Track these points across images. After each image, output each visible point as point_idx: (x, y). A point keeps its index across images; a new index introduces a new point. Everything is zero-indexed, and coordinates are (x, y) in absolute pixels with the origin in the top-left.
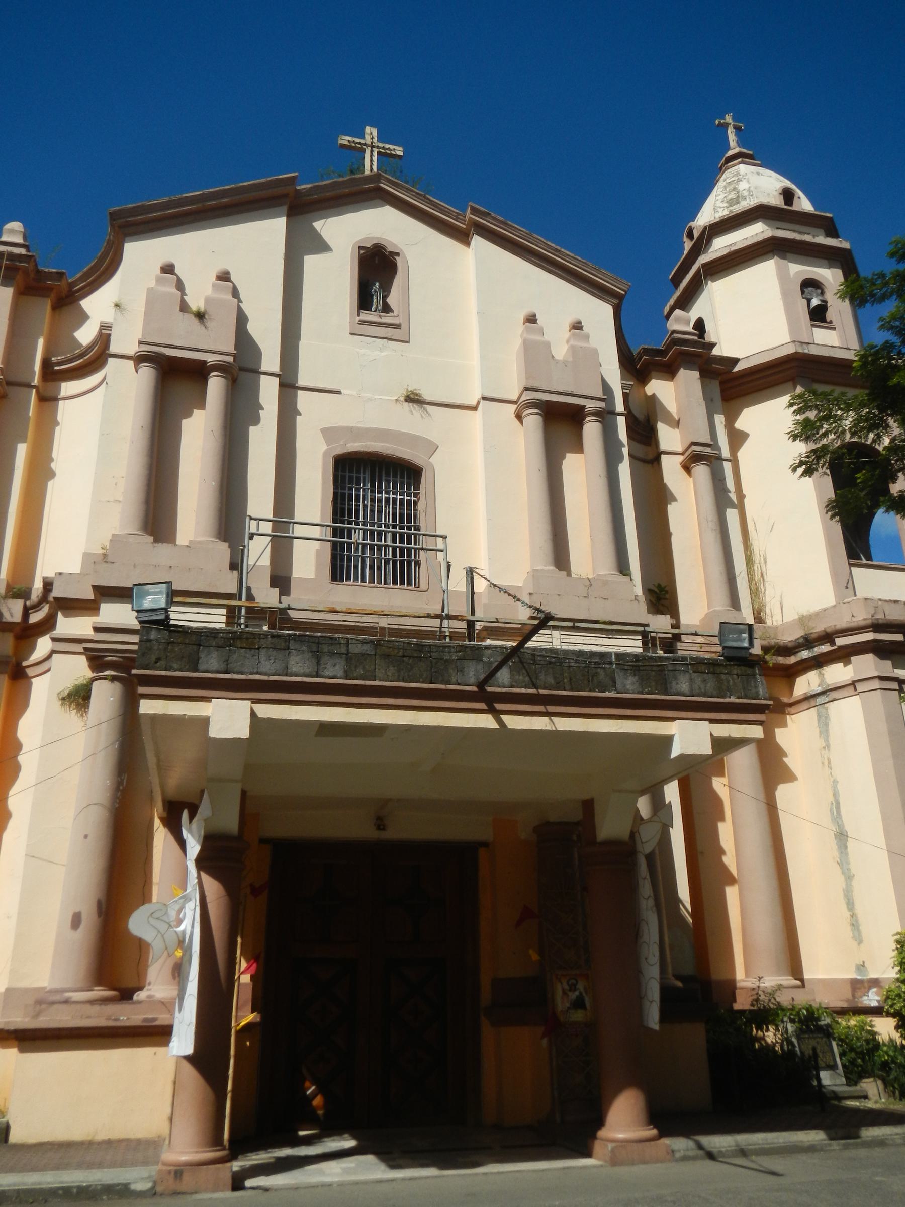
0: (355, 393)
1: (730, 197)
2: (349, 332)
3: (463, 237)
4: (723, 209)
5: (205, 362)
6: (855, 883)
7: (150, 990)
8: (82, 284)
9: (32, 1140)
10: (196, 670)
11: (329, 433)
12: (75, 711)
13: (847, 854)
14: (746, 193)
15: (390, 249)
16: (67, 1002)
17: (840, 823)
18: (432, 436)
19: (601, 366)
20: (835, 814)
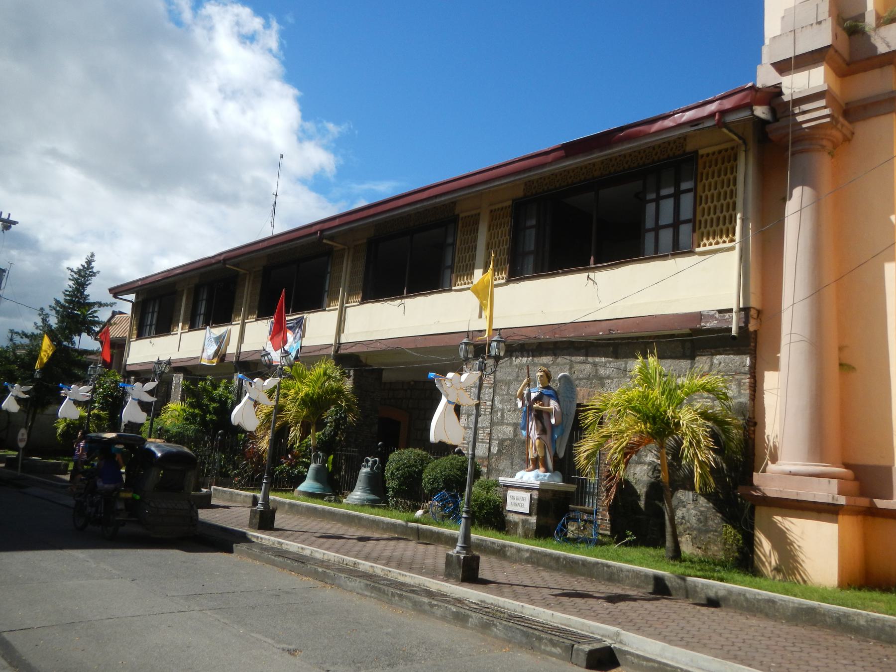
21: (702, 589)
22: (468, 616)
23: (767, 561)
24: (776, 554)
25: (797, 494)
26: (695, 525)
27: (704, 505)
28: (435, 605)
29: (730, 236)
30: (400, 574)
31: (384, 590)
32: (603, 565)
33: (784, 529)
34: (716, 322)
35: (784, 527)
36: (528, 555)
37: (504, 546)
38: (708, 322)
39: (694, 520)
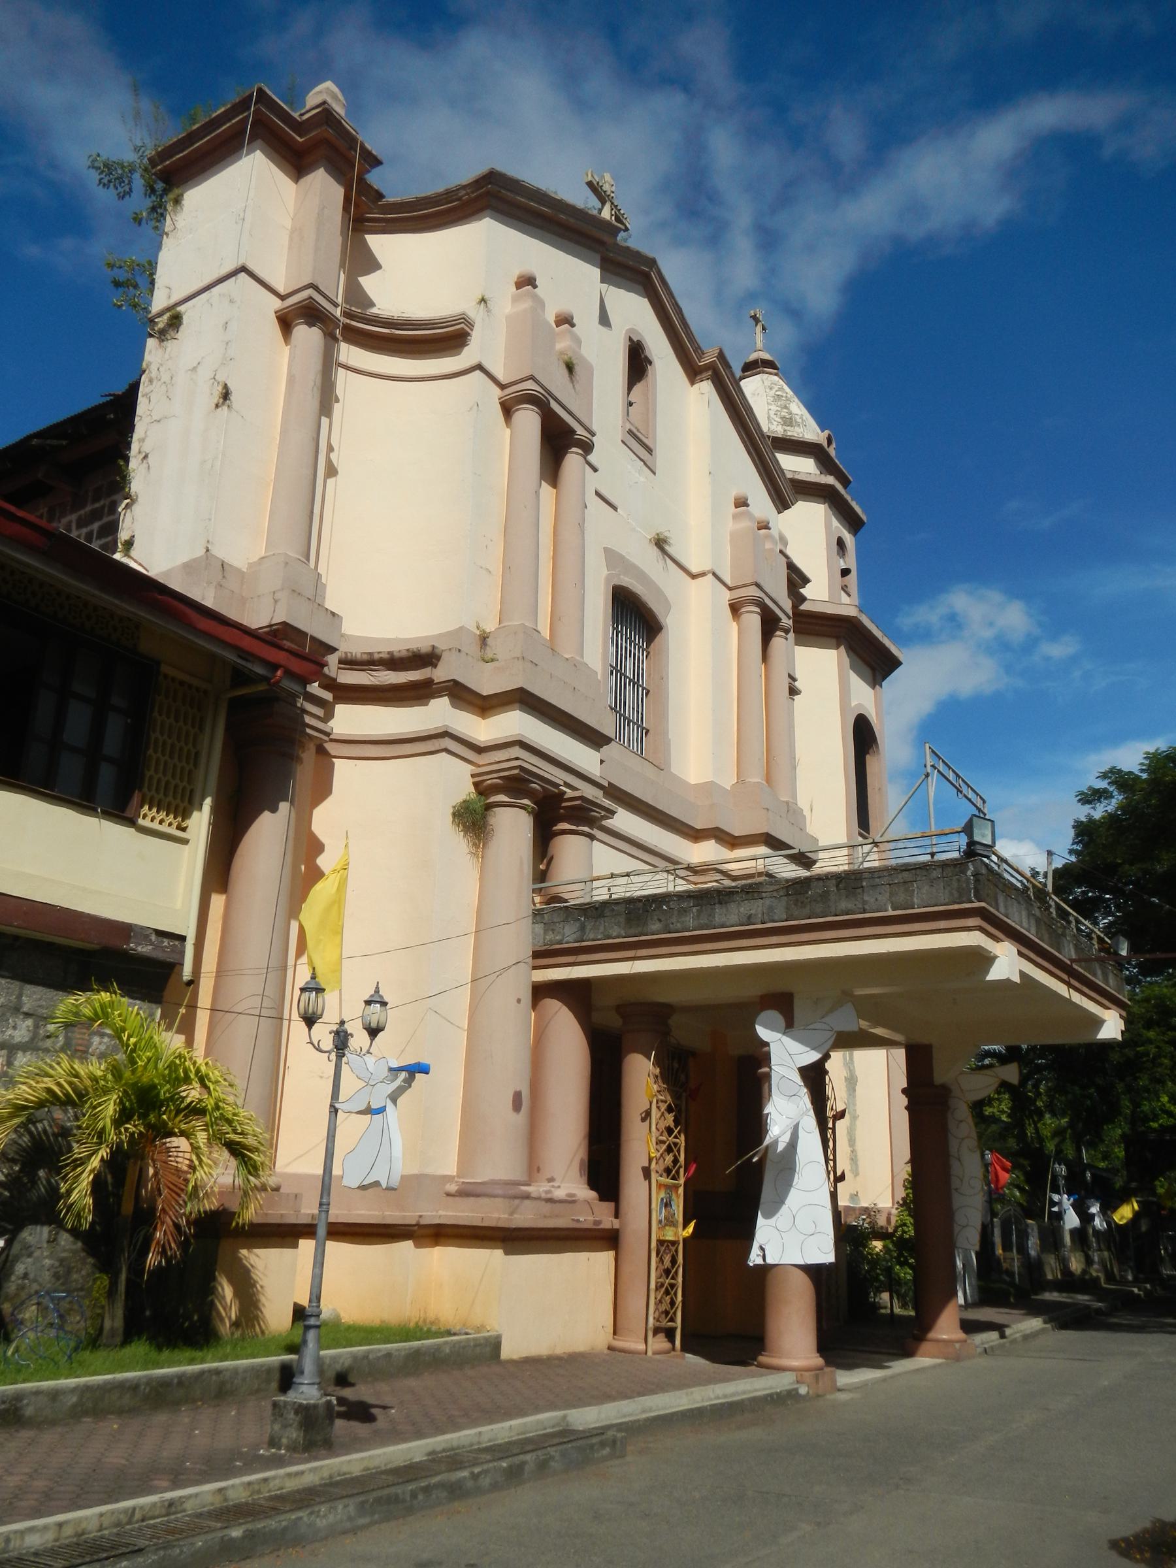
0: (625, 516)
1: (783, 414)
2: (619, 438)
3: (693, 372)
4: (775, 423)
5: (573, 432)
6: (858, 1123)
7: (559, 1187)
8: (378, 216)
9: (515, 1357)
10: (998, 910)
11: (612, 557)
12: (462, 833)
13: (854, 1097)
14: (800, 421)
15: (648, 354)
16: (527, 1197)
17: (852, 1068)
18: (669, 593)
19: (586, 507)
20: (848, 1059)
21: (330, 1365)
22: (524, 1463)
23: (226, 1314)
24: (237, 1302)
25: (282, 1215)
26: (49, 1285)
27: (67, 1247)
28: (480, 1474)
29: (180, 819)
30: (289, 1475)
31: (397, 1495)
32: (210, 1371)
33: (249, 1266)
34: (150, 947)
35: (250, 1263)
36: (74, 1399)
37: (19, 1397)
38: (140, 944)
39: (47, 1276)
